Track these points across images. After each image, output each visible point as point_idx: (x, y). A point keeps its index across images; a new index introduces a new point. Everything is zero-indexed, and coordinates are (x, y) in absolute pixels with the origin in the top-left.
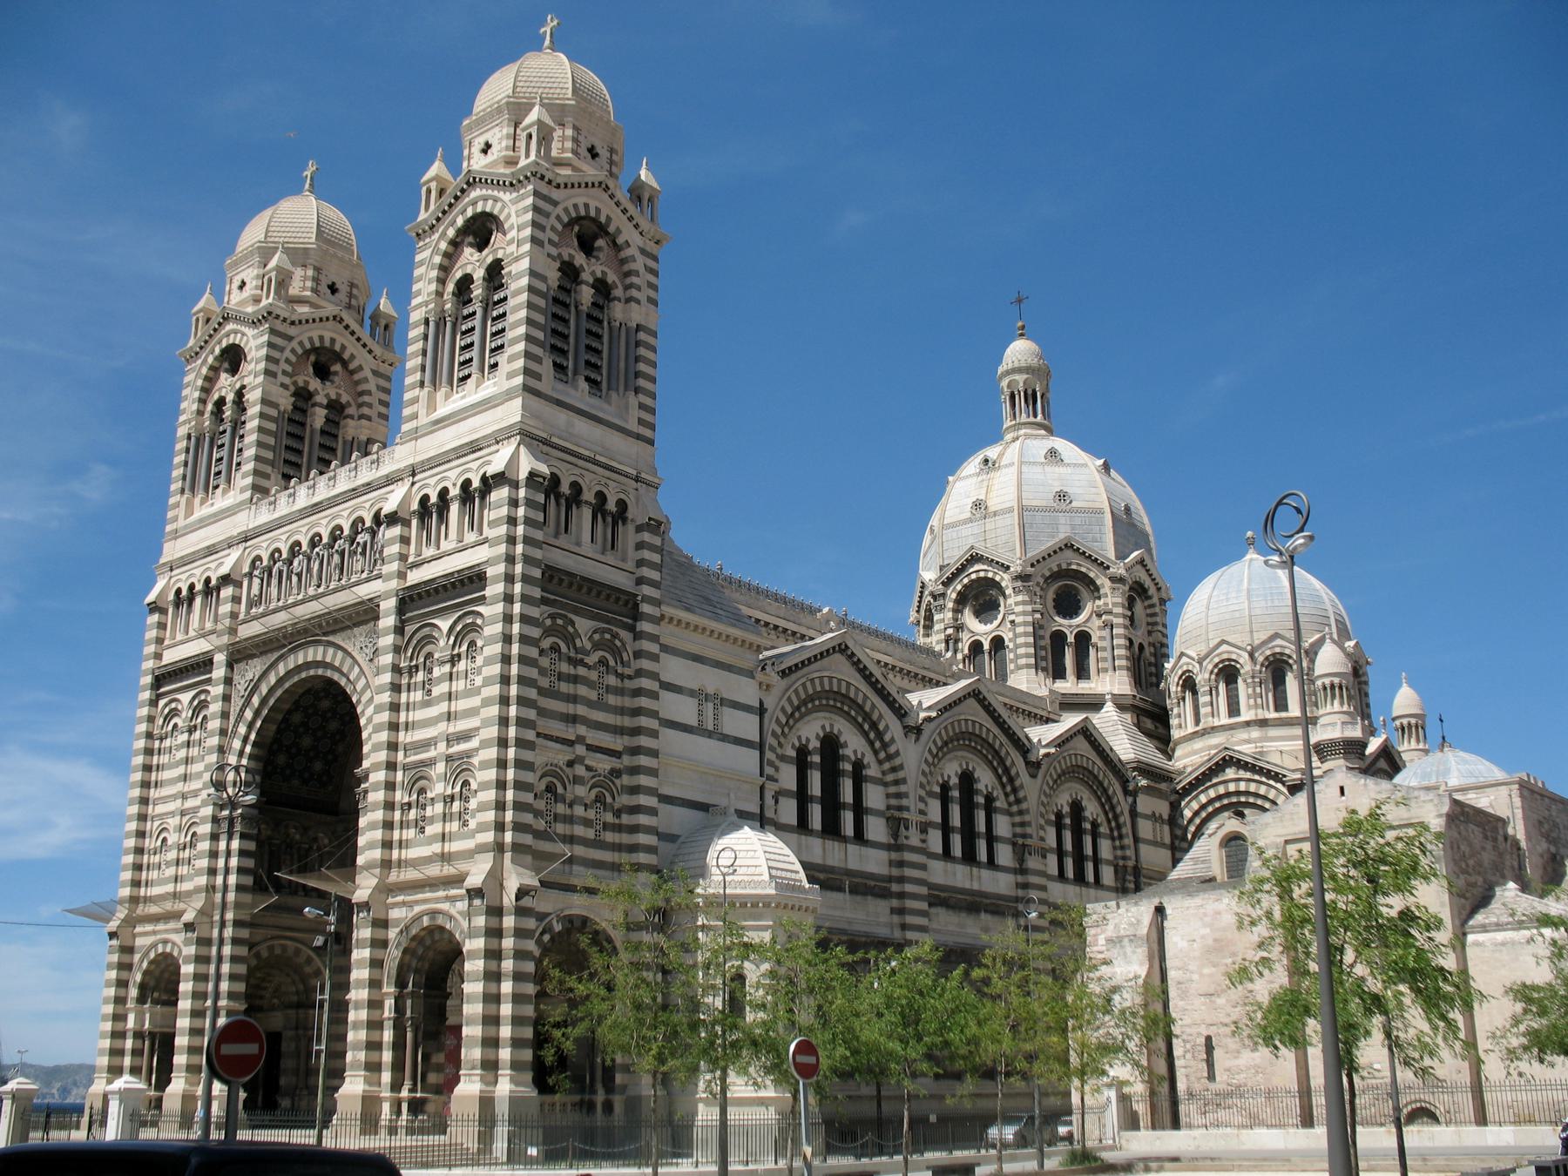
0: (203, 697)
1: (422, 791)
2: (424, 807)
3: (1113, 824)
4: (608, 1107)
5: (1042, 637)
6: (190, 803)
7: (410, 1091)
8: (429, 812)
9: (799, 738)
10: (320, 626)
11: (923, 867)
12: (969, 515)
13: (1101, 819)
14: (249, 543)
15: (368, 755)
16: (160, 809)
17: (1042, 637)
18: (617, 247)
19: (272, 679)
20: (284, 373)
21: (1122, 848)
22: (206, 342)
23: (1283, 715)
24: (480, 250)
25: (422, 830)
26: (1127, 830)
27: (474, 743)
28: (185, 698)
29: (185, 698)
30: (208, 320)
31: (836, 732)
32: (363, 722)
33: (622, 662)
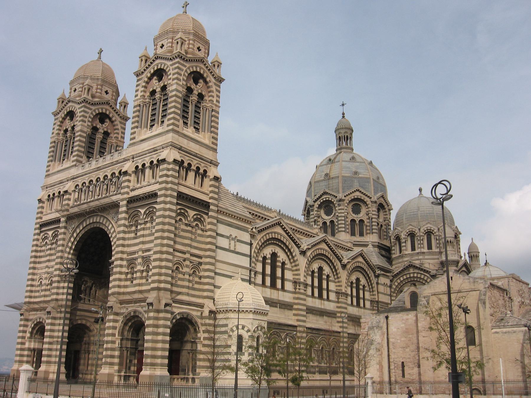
1: (132, 268)
2: (133, 274)
3: (370, 287)
4: (193, 380)
5: (347, 221)
6: (51, 270)
7: (125, 373)
8: (135, 276)
9: (263, 254)
10: (99, 209)
11: (305, 300)
12: (323, 178)
13: (366, 285)
14: (74, 180)
15: (114, 255)
17: (347, 221)
18: (206, 82)
20: (89, 121)
21: (373, 295)
22: (62, 109)
23: (430, 251)
24: (159, 82)
25: (132, 282)
26: (375, 289)
27: (152, 252)
28: (50, 233)
29: (50, 233)
30: (63, 102)
31: (276, 252)
32: (112, 243)
33: (204, 226)
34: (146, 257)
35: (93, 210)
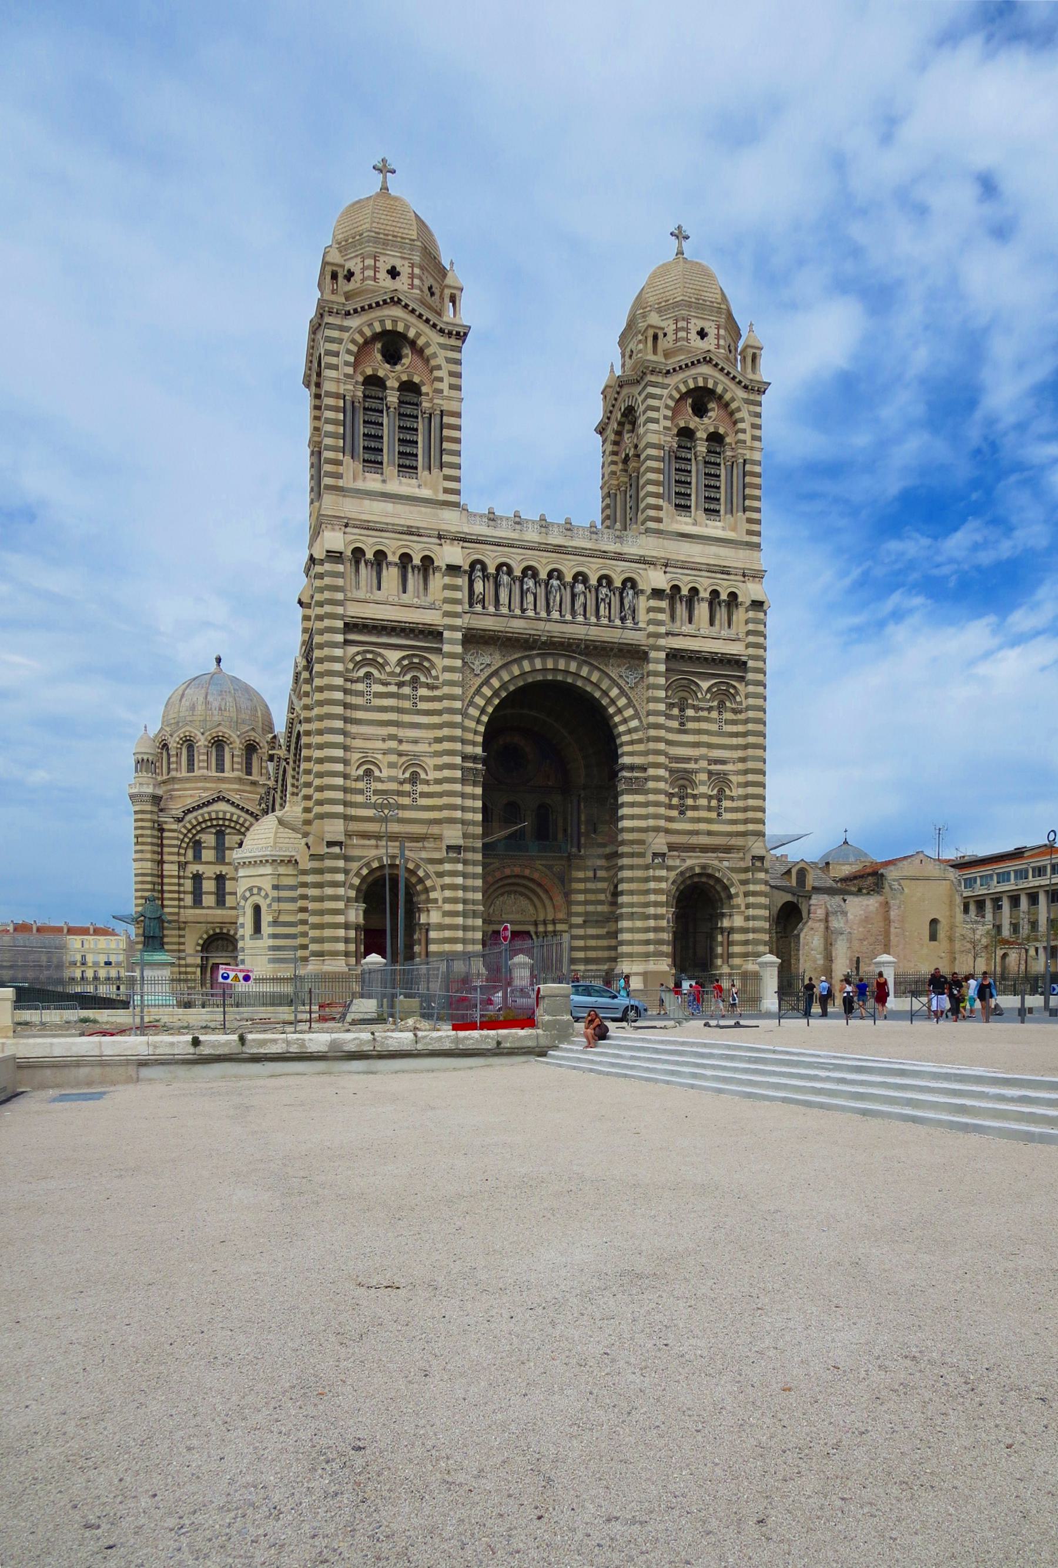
0: (416, 660)
10: (578, 646)
14: (466, 545)
16: (357, 743)
19: (516, 671)
25: (682, 813)
28: (393, 656)
34: (717, 774)
35: (570, 645)
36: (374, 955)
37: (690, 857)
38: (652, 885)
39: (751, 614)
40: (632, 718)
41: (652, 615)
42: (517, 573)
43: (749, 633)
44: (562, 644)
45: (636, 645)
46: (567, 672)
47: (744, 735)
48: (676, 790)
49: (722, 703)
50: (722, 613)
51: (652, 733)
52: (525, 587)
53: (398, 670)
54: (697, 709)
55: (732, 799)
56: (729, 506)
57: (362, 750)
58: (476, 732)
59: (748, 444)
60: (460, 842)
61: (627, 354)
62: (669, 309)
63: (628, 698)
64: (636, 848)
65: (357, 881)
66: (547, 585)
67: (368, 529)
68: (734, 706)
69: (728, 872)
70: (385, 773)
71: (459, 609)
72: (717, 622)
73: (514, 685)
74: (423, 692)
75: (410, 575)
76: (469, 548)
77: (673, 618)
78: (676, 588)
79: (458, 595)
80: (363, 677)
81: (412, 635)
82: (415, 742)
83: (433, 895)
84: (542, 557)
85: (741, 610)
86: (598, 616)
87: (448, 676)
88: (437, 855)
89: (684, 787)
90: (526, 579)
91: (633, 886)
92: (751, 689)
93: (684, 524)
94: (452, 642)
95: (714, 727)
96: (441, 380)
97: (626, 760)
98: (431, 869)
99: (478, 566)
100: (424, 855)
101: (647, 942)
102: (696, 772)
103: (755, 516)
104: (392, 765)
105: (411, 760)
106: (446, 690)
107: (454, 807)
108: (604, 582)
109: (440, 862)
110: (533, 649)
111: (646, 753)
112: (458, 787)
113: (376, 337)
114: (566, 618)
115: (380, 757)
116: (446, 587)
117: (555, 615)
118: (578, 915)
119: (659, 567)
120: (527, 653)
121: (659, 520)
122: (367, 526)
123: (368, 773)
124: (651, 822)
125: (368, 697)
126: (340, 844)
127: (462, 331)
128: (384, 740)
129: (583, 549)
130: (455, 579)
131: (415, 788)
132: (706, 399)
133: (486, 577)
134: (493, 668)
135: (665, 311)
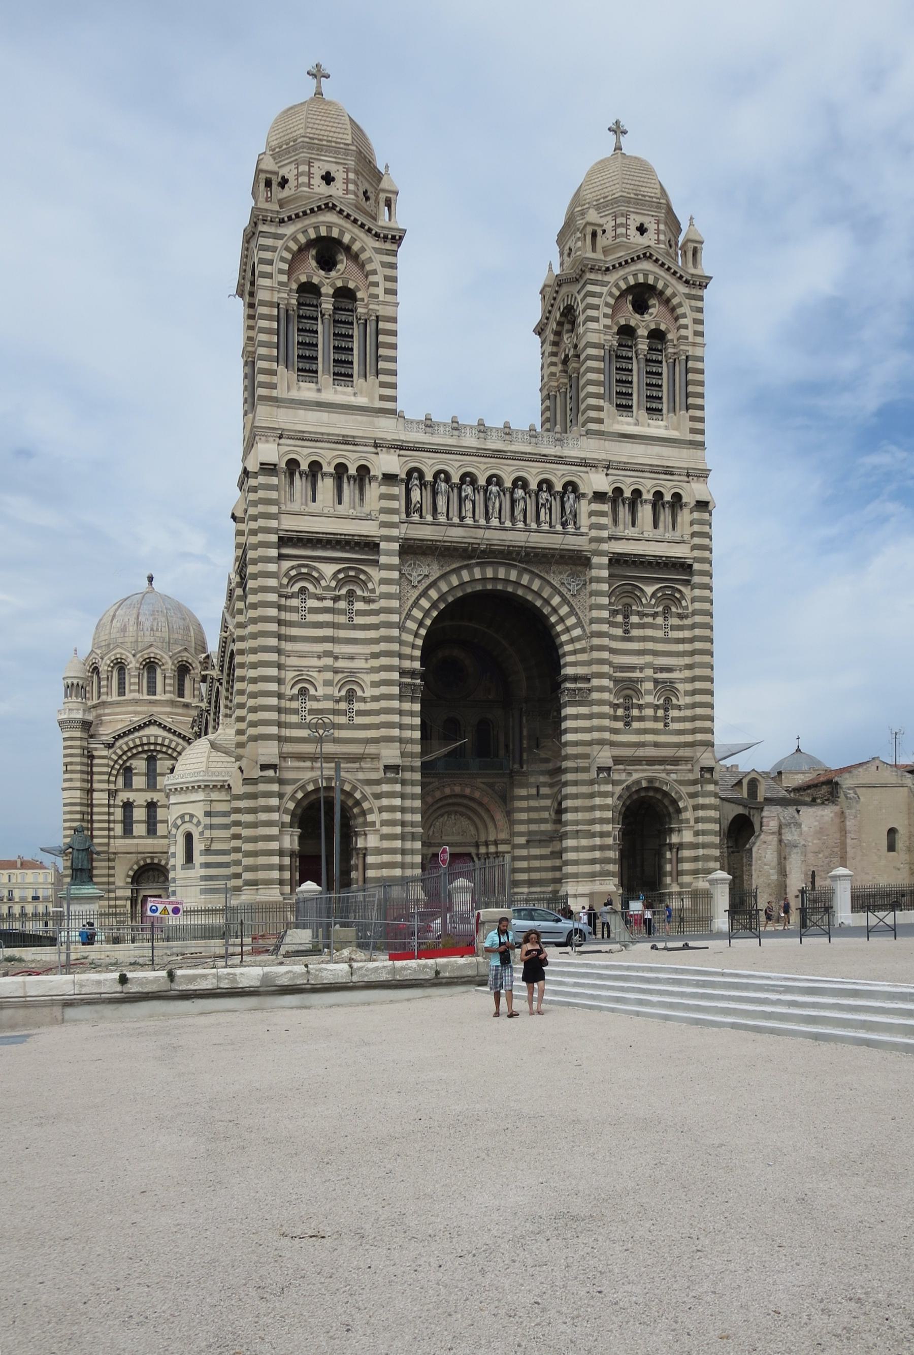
0: (352, 573)
14: (402, 452)
16: (292, 661)
19: (455, 581)
25: (627, 724)
28: (329, 570)
34: (663, 682)
35: (510, 553)
36: (309, 882)
37: (636, 770)
38: (598, 801)
39: (696, 515)
40: (574, 627)
41: (594, 519)
42: (456, 479)
43: (693, 535)
44: (501, 552)
45: (578, 551)
46: (507, 581)
47: (692, 640)
48: (621, 700)
49: (667, 609)
50: (665, 516)
51: (596, 641)
52: (463, 494)
53: (333, 584)
54: (642, 615)
55: (679, 708)
56: (672, 405)
57: (298, 668)
58: (414, 646)
59: (691, 340)
60: (398, 761)
61: (566, 253)
62: (607, 206)
63: (571, 606)
64: (582, 763)
65: (291, 805)
66: (486, 491)
67: (303, 440)
68: (680, 611)
69: (676, 786)
70: (321, 692)
71: (395, 518)
72: (661, 525)
73: (453, 596)
74: (359, 605)
75: (345, 485)
76: (406, 456)
77: (615, 521)
78: (618, 491)
79: (395, 504)
80: (298, 592)
81: (348, 548)
82: (351, 658)
83: (370, 818)
84: (480, 463)
85: (686, 511)
86: (538, 521)
87: (384, 589)
88: (374, 776)
89: (629, 697)
90: (464, 486)
91: (578, 803)
92: (697, 592)
93: (625, 424)
94: (389, 553)
95: (659, 634)
96: (376, 284)
97: (569, 671)
98: (368, 790)
99: (415, 475)
100: (361, 776)
101: (593, 862)
102: (641, 681)
103: (698, 413)
104: (327, 683)
105: (347, 677)
106: (383, 603)
107: (390, 725)
108: (544, 487)
109: (378, 782)
110: (471, 558)
111: (590, 663)
112: (395, 704)
113: (311, 243)
114: (506, 525)
115: (315, 674)
116: (383, 497)
117: (495, 522)
118: (521, 834)
119: (600, 469)
120: (465, 563)
121: (600, 421)
122: (301, 437)
123: (303, 692)
124: (596, 735)
125: (303, 613)
126: (273, 767)
127: (397, 234)
128: (319, 657)
129: (522, 453)
130: (391, 488)
131: (351, 706)
132: (647, 296)
133: (423, 485)
134: (432, 579)
135: (604, 207)
